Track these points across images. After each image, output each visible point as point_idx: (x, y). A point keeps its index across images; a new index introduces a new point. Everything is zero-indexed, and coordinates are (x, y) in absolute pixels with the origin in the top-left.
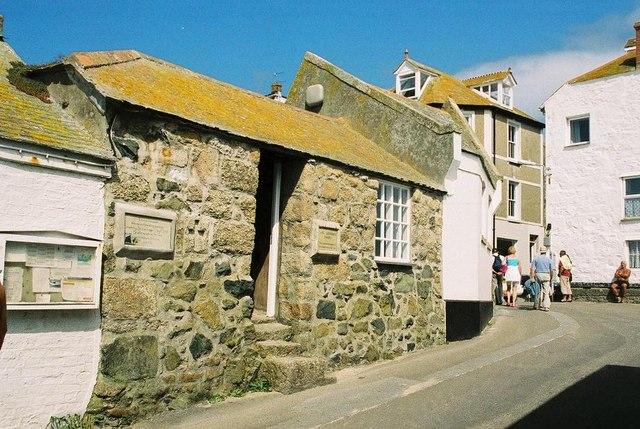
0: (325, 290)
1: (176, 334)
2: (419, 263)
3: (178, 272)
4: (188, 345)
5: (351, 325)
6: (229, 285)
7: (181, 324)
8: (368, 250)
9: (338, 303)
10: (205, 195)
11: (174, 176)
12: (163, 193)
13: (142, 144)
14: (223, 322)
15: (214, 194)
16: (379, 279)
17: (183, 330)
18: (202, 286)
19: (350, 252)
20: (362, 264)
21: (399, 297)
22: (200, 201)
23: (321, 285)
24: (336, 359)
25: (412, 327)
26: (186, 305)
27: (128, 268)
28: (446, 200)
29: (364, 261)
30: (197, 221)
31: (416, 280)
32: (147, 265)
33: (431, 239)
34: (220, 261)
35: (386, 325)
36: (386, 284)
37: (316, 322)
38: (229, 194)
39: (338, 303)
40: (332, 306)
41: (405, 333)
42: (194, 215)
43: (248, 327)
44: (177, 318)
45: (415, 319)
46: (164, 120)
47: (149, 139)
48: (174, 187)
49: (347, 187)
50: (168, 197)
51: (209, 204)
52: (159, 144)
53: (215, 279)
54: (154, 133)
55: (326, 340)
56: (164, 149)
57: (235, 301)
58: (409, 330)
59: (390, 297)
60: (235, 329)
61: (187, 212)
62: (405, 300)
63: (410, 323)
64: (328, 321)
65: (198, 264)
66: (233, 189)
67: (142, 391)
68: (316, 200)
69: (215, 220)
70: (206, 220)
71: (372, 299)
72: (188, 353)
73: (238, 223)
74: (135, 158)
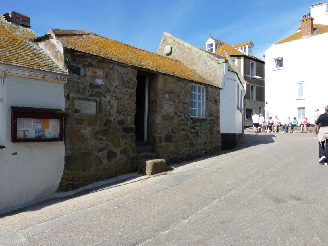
4: (105, 155)
5: (180, 144)
9: (173, 135)
10: (112, 90)
11: (99, 82)
15: (116, 89)
16: (192, 125)
21: (201, 132)
25: (207, 145)
26: (104, 138)
28: (221, 91)
29: (185, 117)
33: (214, 107)
34: (120, 119)
36: (195, 127)
37: (164, 143)
38: (124, 90)
40: (171, 137)
41: (204, 147)
44: (100, 144)
45: (208, 141)
46: (91, 57)
47: (85, 66)
48: (98, 86)
50: (95, 91)
51: (114, 94)
52: (91, 69)
54: (88, 63)
56: (92, 70)
59: (197, 132)
61: (104, 98)
63: (205, 143)
65: (110, 120)
69: (117, 101)
71: (189, 134)
73: (128, 102)
74: (79, 74)
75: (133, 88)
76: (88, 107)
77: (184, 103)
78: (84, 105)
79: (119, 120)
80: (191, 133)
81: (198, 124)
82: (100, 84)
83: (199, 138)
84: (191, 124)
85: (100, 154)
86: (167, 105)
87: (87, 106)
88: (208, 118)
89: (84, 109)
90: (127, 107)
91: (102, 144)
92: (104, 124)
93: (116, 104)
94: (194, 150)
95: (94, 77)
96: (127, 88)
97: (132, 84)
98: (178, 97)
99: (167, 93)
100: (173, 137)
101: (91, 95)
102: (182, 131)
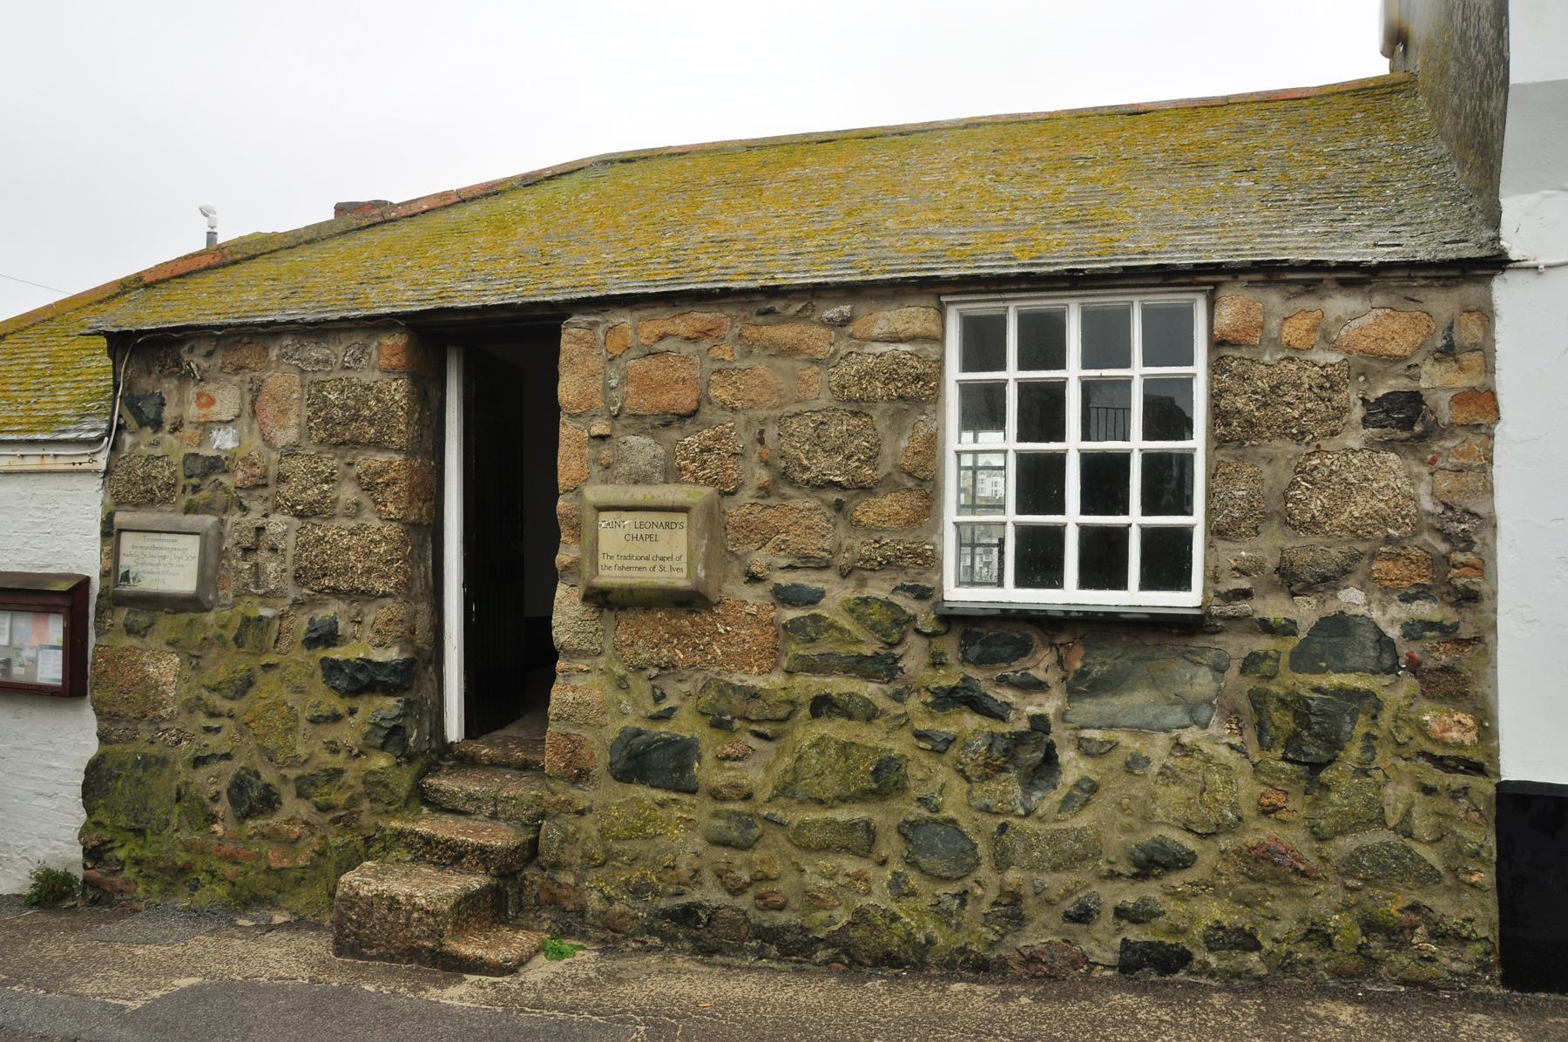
0: (658, 699)
1: (198, 762)
2: (1273, 608)
3: (220, 636)
4: (223, 786)
6: (332, 669)
7: (215, 743)
9: (710, 743)
11: (224, 441)
12: (195, 481)
13: (168, 386)
14: (301, 750)
17: (214, 755)
18: (268, 667)
20: (846, 622)
22: (265, 486)
23: (641, 686)
24: (686, 916)
25: (1176, 880)
27: (130, 630)
28: (1505, 291)
30: (260, 530)
32: (167, 624)
35: (983, 849)
38: (330, 462)
39: (710, 743)
40: (683, 751)
41: (1129, 895)
42: (254, 518)
43: (373, 773)
44: (208, 730)
48: (215, 465)
51: (284, 488)
53: (300, 654)
56: (199, 395)
57: (340, 705)
58: (1151, 890)
60: (338, 772)
64: (660, 795)
65: (260, 618)
66: (337, 445)
67: (138, 852)
68: (599, 428)
70: (279, 524)
72: (223, 808)
73: (352, 524)
74: (157, 424)
75: (377, 445)
76: (168, 560)
77: (837, 485)
78: (155, 552)
79: (312, 621)
80: (940, 746)
81: (1041, 664)
82: (226, 450)
83: (1057, 796)
84: (937, 662)
85: (201, 776)
86: (628, 519)
87: (164, 557)
89: (155, 569)
90: (348, 549)
91: (218, 730)
92: (236, 639)
93: (291, 538)
94: (963, 897)
95: (206, 426)
96: (344, 443)
97: (371, 422)
98: (761, 441)
99: (642, 422)
100: (708, 757)
101: (190, 509)
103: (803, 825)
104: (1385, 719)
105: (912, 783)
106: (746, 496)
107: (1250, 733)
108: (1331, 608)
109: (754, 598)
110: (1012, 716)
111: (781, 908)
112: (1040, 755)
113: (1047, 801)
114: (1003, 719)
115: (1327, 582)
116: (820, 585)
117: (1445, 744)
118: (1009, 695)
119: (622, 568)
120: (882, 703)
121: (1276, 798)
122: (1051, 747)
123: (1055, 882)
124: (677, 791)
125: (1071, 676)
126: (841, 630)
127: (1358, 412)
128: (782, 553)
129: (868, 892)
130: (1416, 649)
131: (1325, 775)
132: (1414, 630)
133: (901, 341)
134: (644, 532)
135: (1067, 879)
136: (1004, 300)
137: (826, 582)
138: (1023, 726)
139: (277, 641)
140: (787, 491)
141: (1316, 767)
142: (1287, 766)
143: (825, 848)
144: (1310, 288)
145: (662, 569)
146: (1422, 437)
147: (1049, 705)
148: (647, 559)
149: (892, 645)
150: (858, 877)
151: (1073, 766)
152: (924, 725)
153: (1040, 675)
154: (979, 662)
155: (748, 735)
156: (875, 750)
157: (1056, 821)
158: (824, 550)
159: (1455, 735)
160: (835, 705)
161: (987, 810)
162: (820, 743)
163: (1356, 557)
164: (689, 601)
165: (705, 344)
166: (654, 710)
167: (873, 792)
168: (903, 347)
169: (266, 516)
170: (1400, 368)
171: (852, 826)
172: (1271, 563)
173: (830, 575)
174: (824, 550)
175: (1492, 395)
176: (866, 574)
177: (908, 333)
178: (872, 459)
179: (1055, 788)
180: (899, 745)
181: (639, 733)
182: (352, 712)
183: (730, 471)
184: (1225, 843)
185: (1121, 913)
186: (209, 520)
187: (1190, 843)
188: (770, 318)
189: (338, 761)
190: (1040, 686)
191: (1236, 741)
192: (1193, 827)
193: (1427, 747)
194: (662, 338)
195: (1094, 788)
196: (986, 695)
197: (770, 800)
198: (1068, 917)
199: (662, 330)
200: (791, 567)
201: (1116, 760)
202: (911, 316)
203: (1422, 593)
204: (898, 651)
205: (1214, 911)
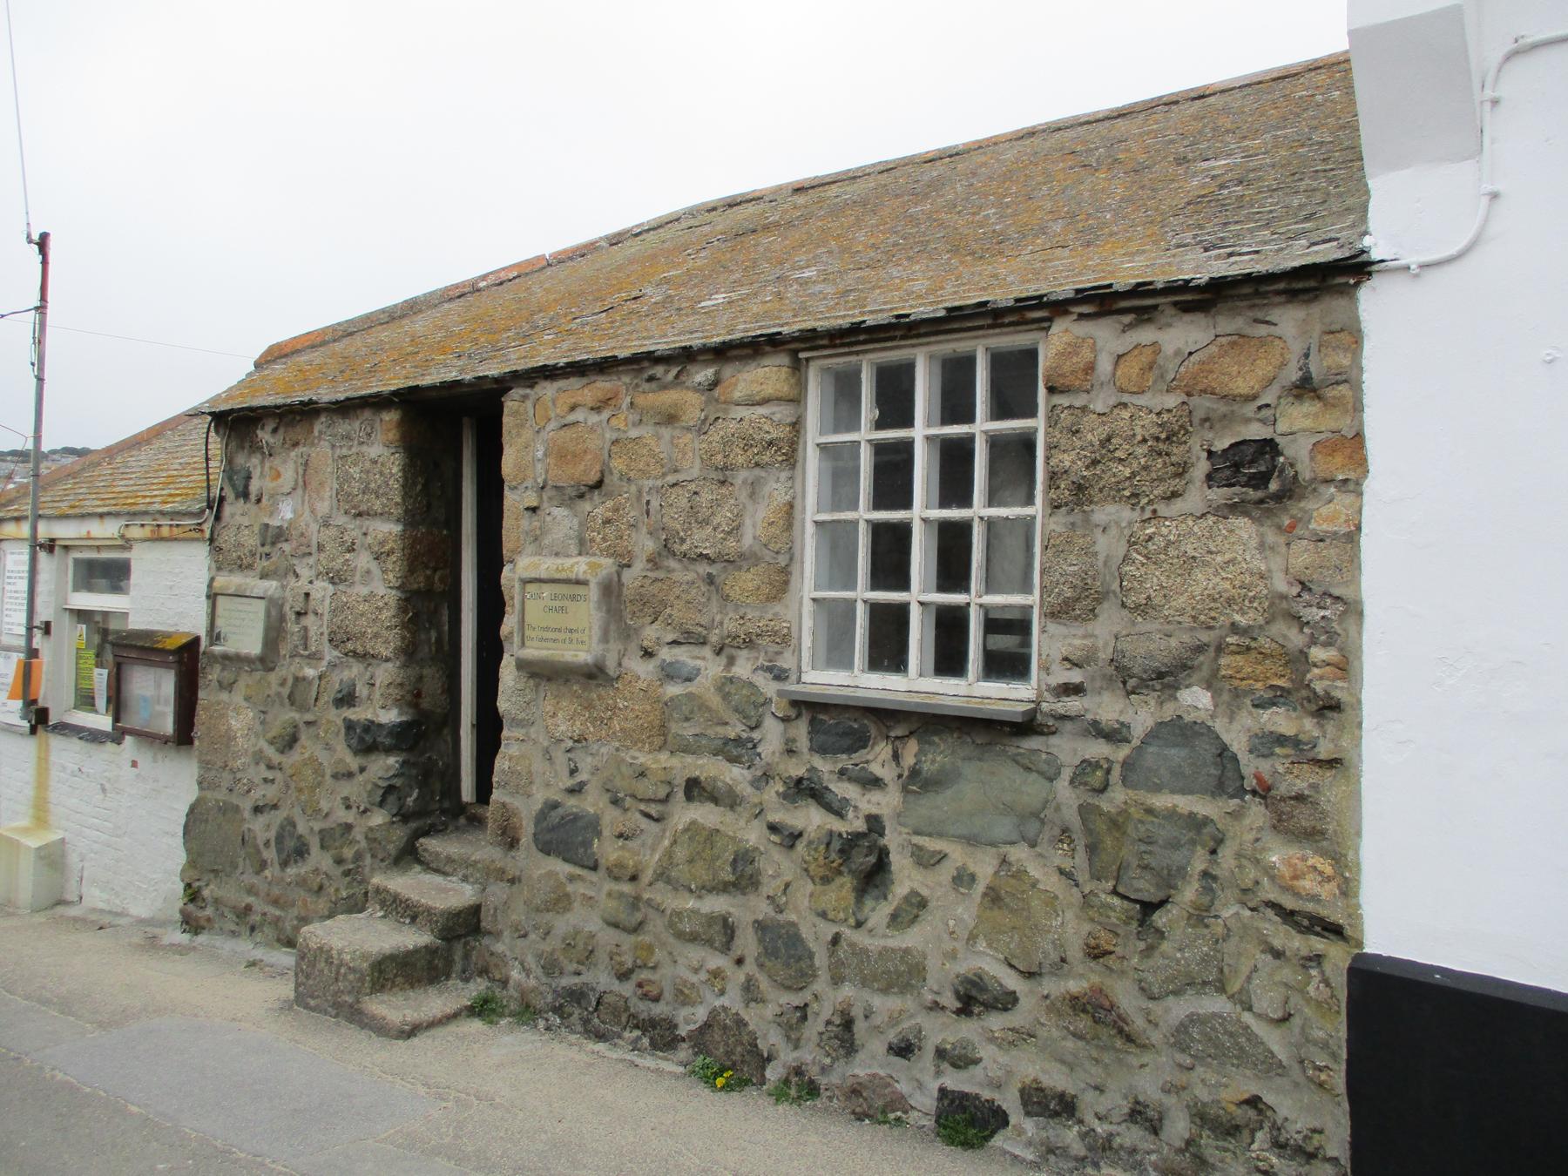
0: (573, 772)
2: (1107, 707)
8: (749, 643)
12: (267, 549)
14: (324, 805)
19: (666, 654)
20: (715, 701)
21: (927, 861)
22: (310, 554)
24: (577, 995)
29: (726, 686)
31: (1066, 795)
35: (821, 960)
38: (353, 529)
39: (611, 819)
49: (633, 433)
55: (563, 924)
58: (968, 1030)
62: (963, 879)
64: (568, 868)
71: (754, 835)
77: (707, 557)
81: (878, 758)
86: (547, 590)
87: (243, 619)
88: (1073, 704)
94: (803, 1009)
102: (689, 797)
103: (678, 914)
104: (1227, 855)
105: (764, 880)
106: (639, 566)
107: (1081, 857)
108: (1169, 711)
109: (643, 670)
110: (851, 815)
111: (656, 999)
112: (872, 859)
113: (878, 913)
114: (840, 814)
115: (1166, 678)
116: (693, 663)
117: (1297, 895)
118: (844, 790)
119: (541, 639)
120: (745, 789)
121: (1105, 942)
122: (883, 854)
123: (885, 1005)
124: (583, 867)
125: (906, 773)
126: (709, 709)
127: (1202, 467)
128: (669, 627)
129: (722, 992)
130: (1265, 766)
131: (1160, 919)
132: (1269, 742)
133: (759, 404)
134: (557, 604)
135: (893, 1003)
136: (857, 353)
137: (704, 659)
138: (860, 825)
139: (316, 700)
140: (672, 563)
141: (1149, 908)
142: (1116, 901)
143: (693, 938)
144: (1145, 315)
145: (571, 641)
146: (1279, 497)
147: (885, 803)
148: (560, 630)
149: (752, 729)
150: (716, 974)
151: (905, 878)
152: (774, 817)
153: (876, 769)
154: (821, 750)
155: (638, 816)
156: (733, 839)
157: (885, 936)
158: (701, 626)
159: (1308, 884)
160: (704, 789)
161: (823, 915)
162: (693, 827)
163: (1200, 649)
164: (594, 674)
165: (606, 414)
166: (570, 783)
167: (734, 885)
168: (761, 410)
169: (311, 582)
170: (1249, 409)
171: (711, 919)
172: (1105, 655)
173: (707, 651)
174: (701, 626)
175: (1359, 437)
176: (733, 651)
177: (762, 395)
178: (735, 530)
179: (885, 898)
180: (754, 835)
181: (555, 806)
182: (362, 770)
183: (626, 543)
184: (1053, 986)
185: (941, 1053)
186: (271, 586)
187: (1012, 981)
188: (654, 385)
189: (350, 817)
190: (875, 783)
191: (1067, 864)
192: (1014, 962)
193: (1273, 896)
194: (573, 408)
195: (923, 904)
196: (827, 788)
197: (650, 884)
198: (891, 1049)
199: (573, 400)
200: (675, 643)
201: (946, 872)
202: (767, 375)
203: (1278, 697)
204: (756, 735)
205: (1032, 1067)
